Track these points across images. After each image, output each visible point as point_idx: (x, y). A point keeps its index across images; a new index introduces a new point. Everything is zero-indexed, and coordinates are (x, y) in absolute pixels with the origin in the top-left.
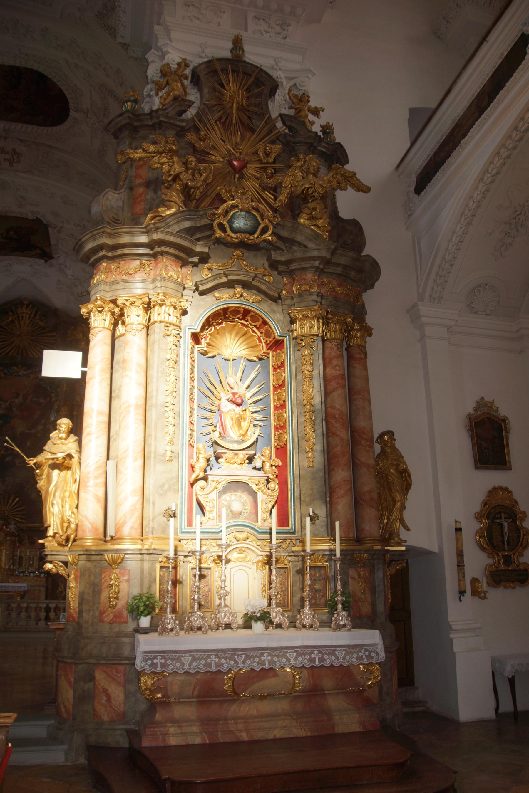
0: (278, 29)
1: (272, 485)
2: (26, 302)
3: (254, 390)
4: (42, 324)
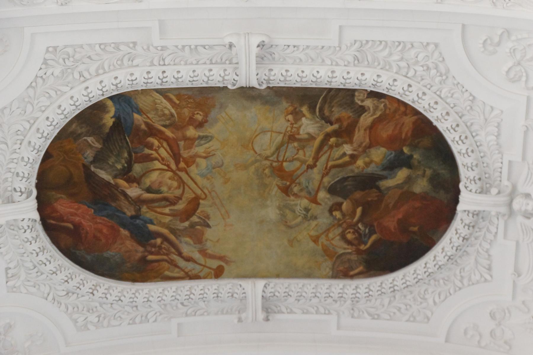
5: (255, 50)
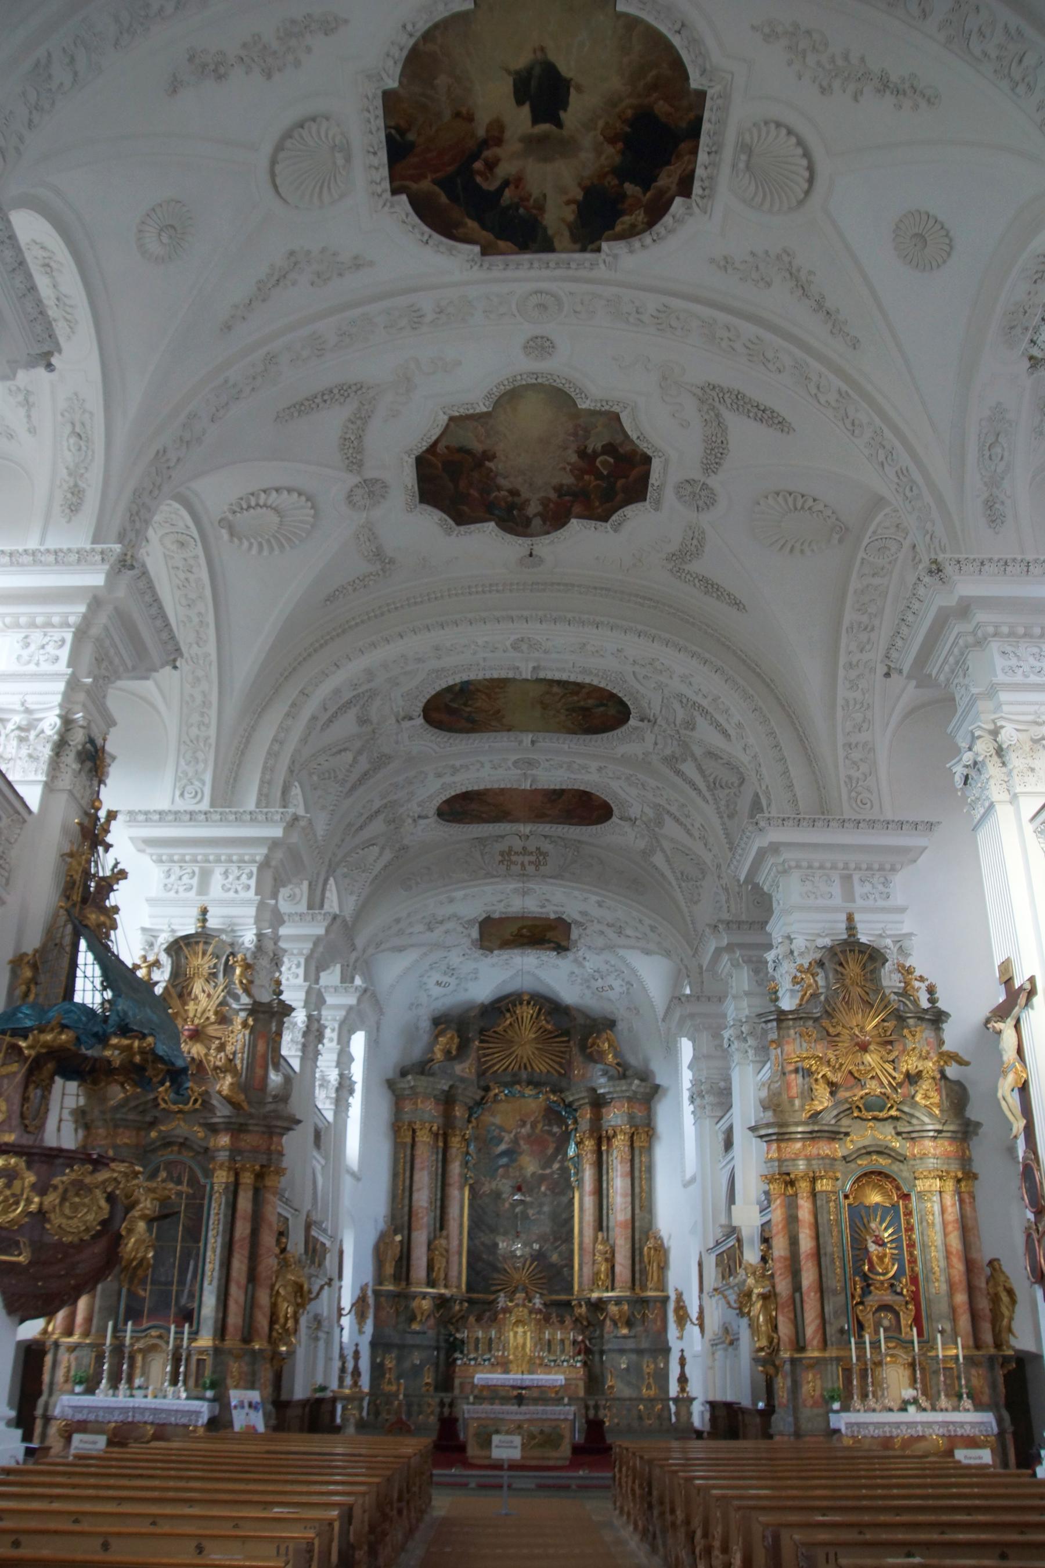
0: (880, 887)
1: (910, 1307)
2: (526, 998)
3: (890, 1231)
4: (549, 1027)
5: (530, 669)
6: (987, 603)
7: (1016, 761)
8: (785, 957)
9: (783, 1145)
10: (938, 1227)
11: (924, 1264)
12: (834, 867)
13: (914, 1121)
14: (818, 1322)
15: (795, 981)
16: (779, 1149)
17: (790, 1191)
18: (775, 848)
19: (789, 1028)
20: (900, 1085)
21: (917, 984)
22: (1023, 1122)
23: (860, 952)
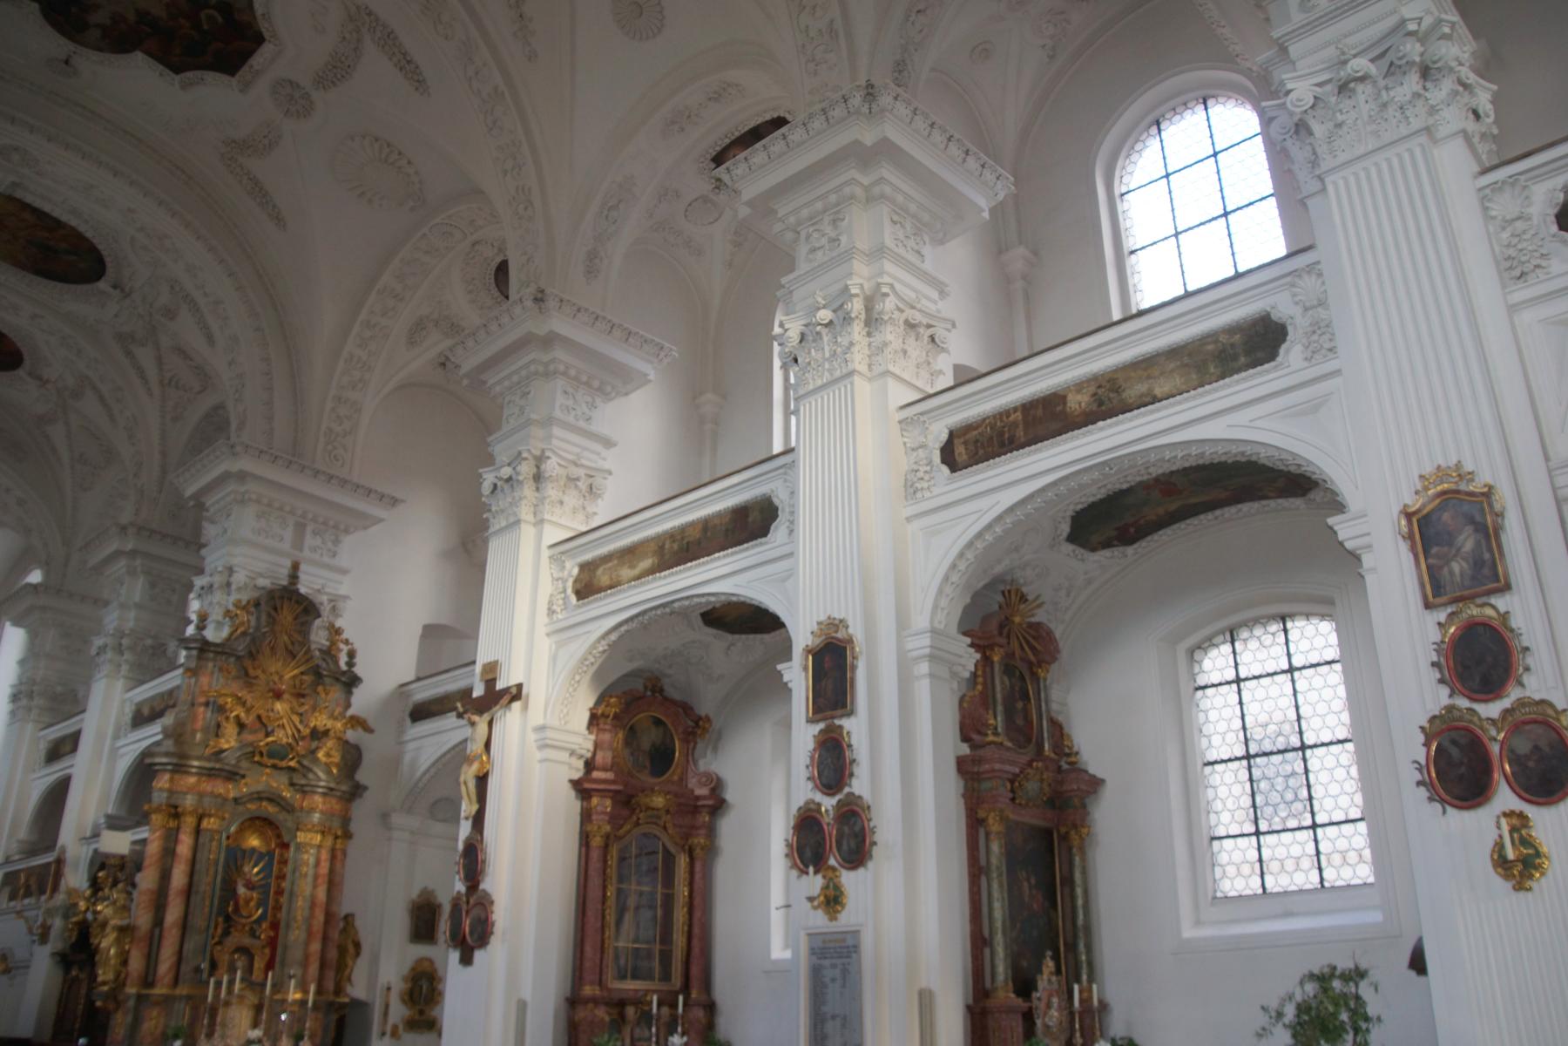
0: (330, 544)
6: (567, 342)
7: (551, 491)
8: (221, 587)
9: (177, 776)
10: (310, 879)
11: (289, 912)
12: (292, 512)
13: (311, 776)
14: (174, 959)
15: (227, 613)
16: (172, 780)
17: (172, 824)
18: (242, 476)
19: (207, 659)
20: (303, 738)
21: (342, 646)
22: (475, 807)
23: (297, 602)
